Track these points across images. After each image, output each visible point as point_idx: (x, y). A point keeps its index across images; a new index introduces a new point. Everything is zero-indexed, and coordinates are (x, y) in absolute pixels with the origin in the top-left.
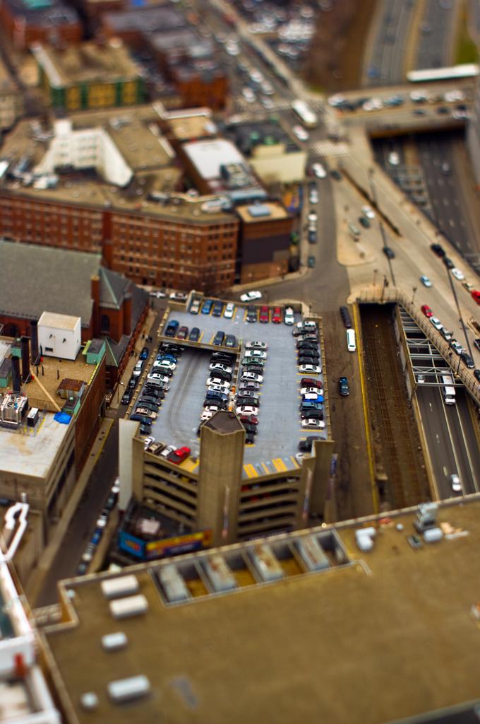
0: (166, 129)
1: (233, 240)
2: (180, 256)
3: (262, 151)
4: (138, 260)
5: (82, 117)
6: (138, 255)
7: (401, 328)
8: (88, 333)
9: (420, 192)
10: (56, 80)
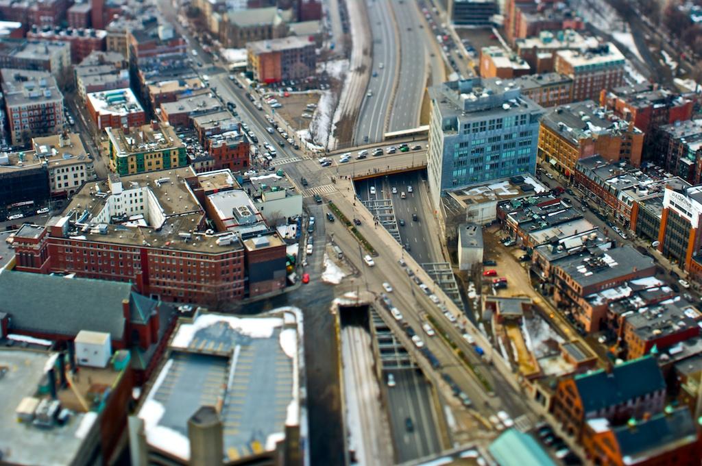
0: (194, 184)
1: (241, 265)
2: (198, 279)
4: (169, 284)
6: (169, 280)
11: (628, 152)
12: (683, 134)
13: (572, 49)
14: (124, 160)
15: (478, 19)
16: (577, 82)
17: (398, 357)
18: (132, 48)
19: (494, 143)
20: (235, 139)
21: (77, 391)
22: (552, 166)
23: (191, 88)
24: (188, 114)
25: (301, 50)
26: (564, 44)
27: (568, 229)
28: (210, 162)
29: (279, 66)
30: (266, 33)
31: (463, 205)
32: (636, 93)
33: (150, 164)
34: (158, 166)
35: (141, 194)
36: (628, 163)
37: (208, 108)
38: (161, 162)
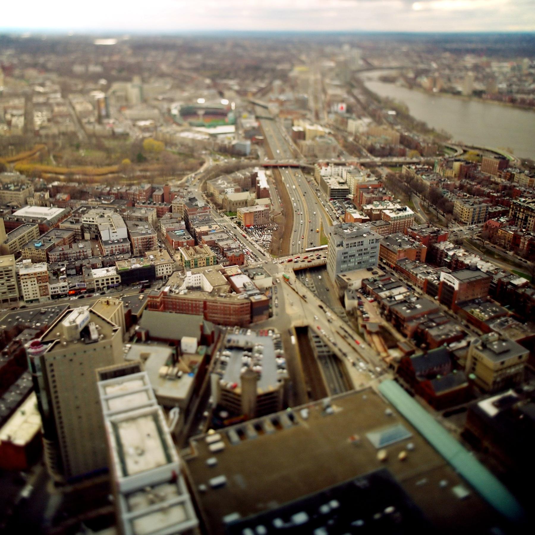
0: (224, 273)
1: (249, 308)
2: (230, 314)
3: (257, 277)
4: (216, 317)
5: (195, 270)
7: (311, 335)
8: (200, 344)
9: (313, 287)
10: (186, 258)
11: (420, 256)
12: (445, 247)
13: (389, 209)
14: (189, 262)
15: (341, 196)
16: (393, 224)
17: (324, 349)
18: (185, 211)
19: (360, 252)
20: (238, 252)
21: (184, 363)
22: (384, 263)
23: (214, 229)
24: (214, 241)
25: (263, 211)
26: (385, 207)
27: (395, 292)
28: (227, 263)
29: (253, 219)
30: (244, 204)
31: (346, 281)
32: (421, 229)
34: (204, 264)
36: (420, 261)
37: (224, 238)
38: (205, 263)
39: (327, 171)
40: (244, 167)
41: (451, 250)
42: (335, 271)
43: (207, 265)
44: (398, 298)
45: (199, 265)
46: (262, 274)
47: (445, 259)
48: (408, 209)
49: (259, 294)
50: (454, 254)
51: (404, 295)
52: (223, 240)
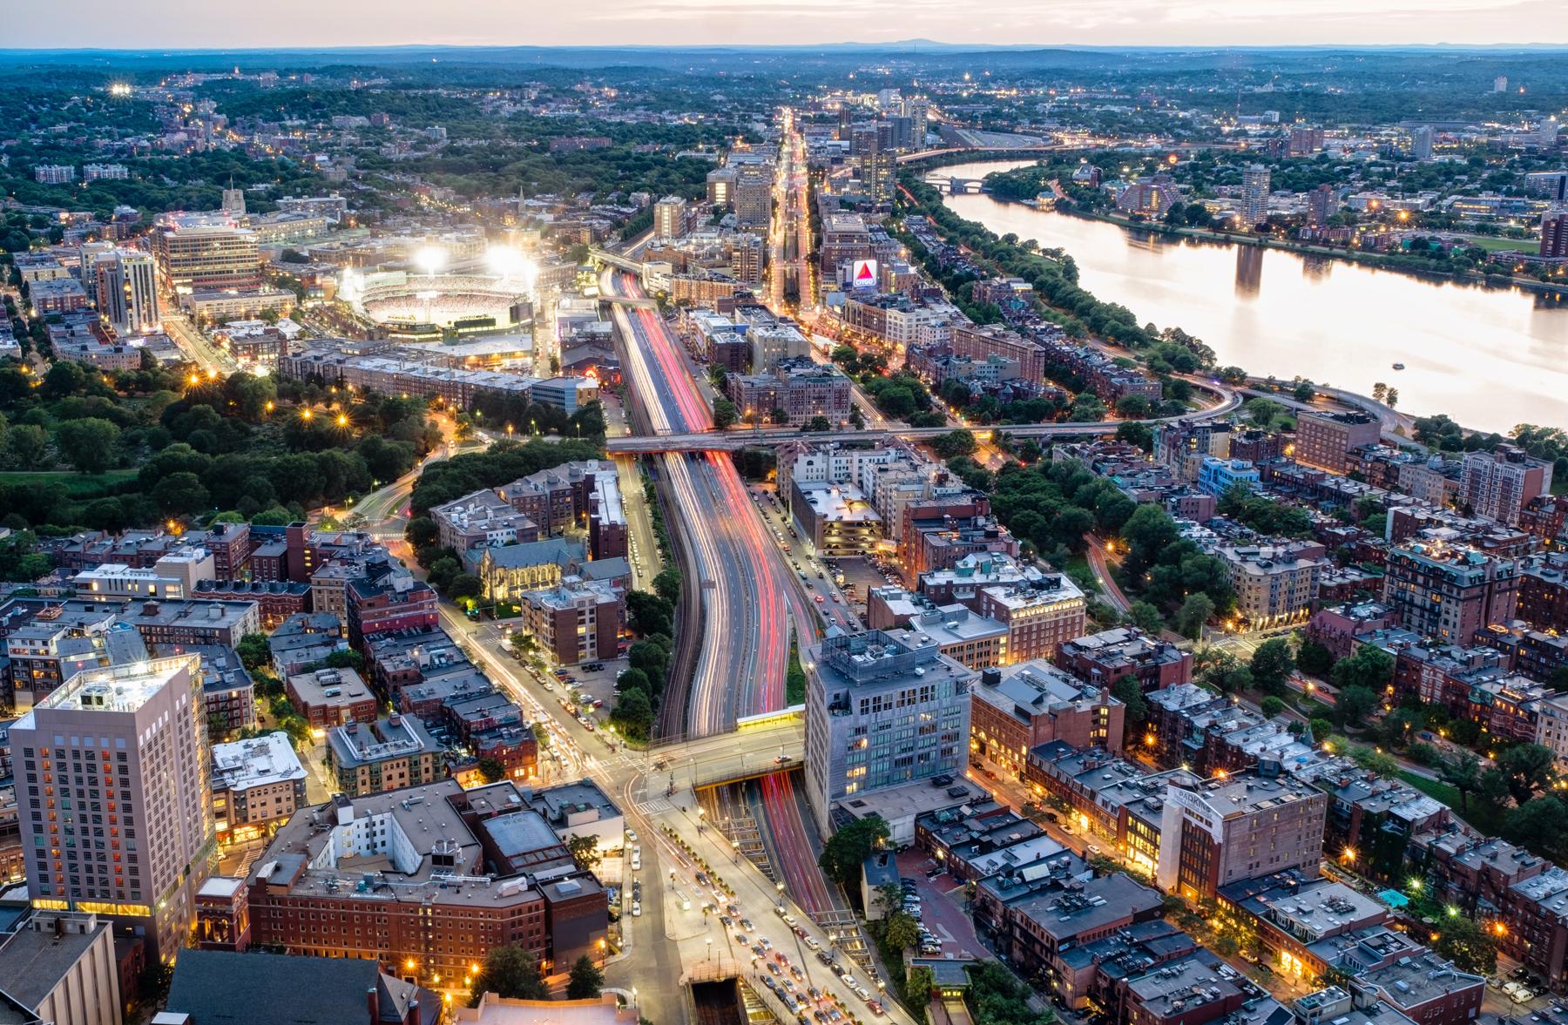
1: (539, 924)
12: (1182, 703)
24: (441, 701)
26: (992, 577)
27: (1024, 853)
33: (390, 778)
35: (382, 822)
38: (407, 775)
39: (814, 467)
40: (551, 459)
41: (1204, 711)
42: (827, 792)
43: (414, 784)
44: (1031, 874)
45: (385, 785)
46: (588, 807)
47: (1187, 742)
48: (1065, 581)
49: (571, 876)
50: (1213, 725)
51: (1053, 863)
52: (468, 698)
